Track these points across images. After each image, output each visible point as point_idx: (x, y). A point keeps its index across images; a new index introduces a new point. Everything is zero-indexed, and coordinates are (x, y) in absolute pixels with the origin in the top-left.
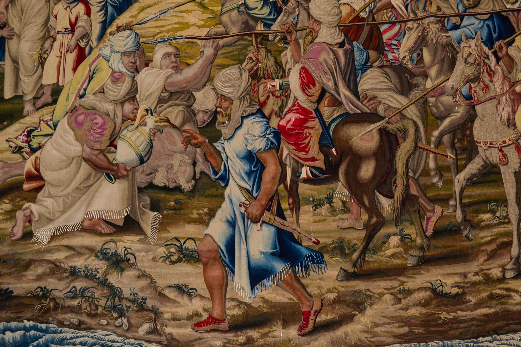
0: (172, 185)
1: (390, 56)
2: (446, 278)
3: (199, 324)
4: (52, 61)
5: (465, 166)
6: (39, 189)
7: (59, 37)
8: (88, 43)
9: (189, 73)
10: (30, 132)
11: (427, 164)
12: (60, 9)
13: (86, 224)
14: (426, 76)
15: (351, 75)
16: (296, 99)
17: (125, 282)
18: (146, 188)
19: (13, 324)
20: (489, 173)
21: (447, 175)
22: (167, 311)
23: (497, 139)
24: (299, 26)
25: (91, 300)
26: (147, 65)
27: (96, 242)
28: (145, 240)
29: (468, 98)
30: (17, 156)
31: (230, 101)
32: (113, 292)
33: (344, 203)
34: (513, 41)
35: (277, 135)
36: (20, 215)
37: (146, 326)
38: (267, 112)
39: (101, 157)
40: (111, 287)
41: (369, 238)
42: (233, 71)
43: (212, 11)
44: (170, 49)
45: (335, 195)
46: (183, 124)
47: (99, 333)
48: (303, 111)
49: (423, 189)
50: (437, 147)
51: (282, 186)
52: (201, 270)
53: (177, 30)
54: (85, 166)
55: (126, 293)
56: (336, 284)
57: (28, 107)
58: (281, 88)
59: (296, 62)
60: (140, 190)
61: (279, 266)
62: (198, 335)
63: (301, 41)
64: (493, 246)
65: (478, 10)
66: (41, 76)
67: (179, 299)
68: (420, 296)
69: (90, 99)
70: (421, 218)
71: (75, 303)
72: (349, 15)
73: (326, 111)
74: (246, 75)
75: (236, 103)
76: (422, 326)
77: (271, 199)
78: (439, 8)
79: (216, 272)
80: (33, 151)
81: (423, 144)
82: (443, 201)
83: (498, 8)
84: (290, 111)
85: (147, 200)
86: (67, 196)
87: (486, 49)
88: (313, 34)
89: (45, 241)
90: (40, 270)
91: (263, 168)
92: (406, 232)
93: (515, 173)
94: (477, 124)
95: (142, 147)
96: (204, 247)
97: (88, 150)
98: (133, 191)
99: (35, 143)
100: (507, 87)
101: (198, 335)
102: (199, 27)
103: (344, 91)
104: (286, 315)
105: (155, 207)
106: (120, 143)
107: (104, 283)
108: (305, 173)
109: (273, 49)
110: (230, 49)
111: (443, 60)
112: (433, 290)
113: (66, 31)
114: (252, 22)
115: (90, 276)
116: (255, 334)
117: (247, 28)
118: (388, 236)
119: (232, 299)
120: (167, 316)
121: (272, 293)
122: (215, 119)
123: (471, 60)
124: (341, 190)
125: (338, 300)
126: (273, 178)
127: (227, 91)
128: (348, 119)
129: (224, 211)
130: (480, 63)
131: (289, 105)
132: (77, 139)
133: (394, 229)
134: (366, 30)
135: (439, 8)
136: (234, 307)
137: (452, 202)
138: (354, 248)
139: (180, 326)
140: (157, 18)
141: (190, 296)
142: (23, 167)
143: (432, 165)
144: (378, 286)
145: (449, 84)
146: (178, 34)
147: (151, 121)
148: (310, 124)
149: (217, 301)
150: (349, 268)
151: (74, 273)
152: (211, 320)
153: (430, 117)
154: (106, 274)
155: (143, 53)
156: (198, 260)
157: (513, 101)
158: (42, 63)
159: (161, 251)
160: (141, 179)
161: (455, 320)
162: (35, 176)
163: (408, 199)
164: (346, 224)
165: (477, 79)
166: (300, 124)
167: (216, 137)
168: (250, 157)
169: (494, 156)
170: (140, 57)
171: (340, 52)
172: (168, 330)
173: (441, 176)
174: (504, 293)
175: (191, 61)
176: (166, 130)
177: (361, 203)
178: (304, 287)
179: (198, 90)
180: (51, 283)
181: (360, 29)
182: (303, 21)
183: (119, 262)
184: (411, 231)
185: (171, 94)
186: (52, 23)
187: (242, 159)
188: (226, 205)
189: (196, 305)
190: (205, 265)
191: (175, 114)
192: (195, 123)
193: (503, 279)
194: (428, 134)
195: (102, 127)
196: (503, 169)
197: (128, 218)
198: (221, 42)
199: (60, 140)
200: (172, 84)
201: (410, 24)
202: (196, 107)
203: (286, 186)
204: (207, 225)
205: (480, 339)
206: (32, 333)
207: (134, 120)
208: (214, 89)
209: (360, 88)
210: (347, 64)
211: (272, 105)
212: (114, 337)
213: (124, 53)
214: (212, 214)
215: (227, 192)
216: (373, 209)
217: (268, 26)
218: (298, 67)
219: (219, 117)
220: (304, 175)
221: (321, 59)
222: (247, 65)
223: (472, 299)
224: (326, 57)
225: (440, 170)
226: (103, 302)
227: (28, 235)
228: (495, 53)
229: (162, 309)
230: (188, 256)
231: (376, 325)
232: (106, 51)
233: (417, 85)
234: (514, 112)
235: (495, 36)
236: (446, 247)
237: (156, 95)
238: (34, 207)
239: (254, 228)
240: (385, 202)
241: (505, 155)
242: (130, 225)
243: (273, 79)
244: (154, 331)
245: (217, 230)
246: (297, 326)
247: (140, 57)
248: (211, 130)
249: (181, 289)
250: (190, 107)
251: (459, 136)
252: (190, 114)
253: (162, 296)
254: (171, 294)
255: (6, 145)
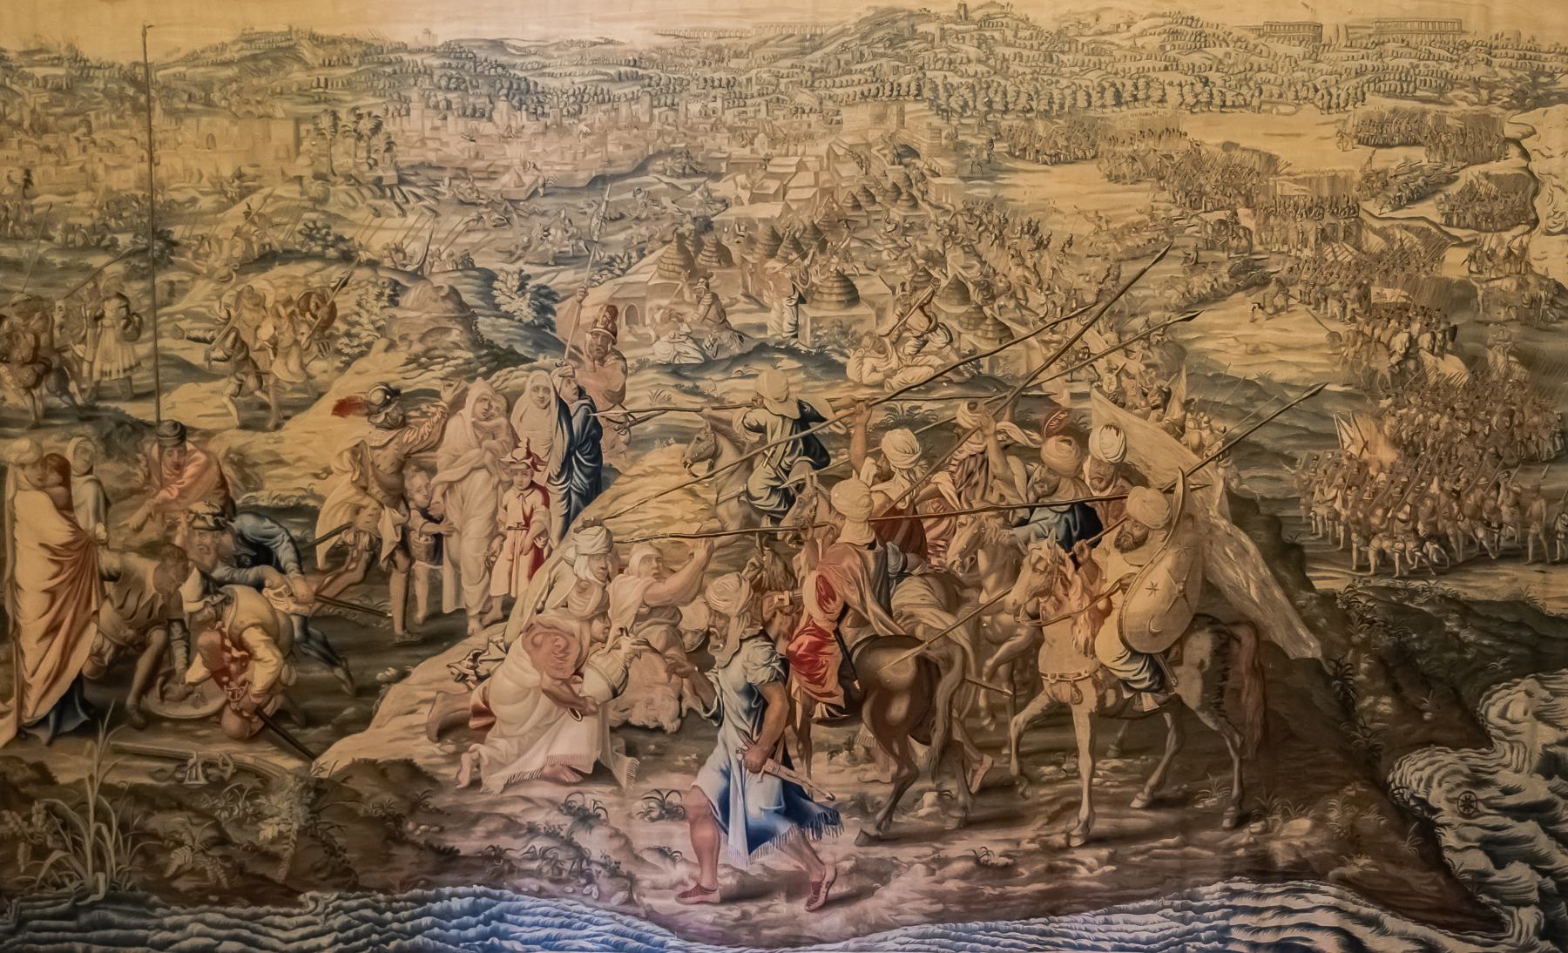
0: (652, 725)
1: (934, 561)
2: (992, 844)
3: (684, 895)
4: (501, 566)
5: (1024, 706)
6: (488, 727)
7: (510, 534)
8: (546, 543)
9: (674, 582)
10: (476, 656)
11: (976, 701)
12: (510, 497)
13: (547, 770)
14: (979, 587)
15: (883, 586)
16: (810, 617)
17: (595, 843)
18: (620, 727)
19: (461, 889)
20: (1058, 715)
21: (1001, 716)
22: (646, 878)
23: (1071, 671)
24: (817, 521)
25: (555, 863)
26: (621, 571)
27: (560, 793)
28: (620, 791)
29: (1035, 616)
30: (461, 687)
31: (727, 618)
32: (581, 854)
33: (868, 750)
34: (1099, 541)
35: (785, 663)
36: (466, 759)
37: (621, 895)
38: (772, 633)
39: (565, 688)
40: (578, 848)
41: (898, 794)
42: (731, 580)
43: (705, 501)
44: (650, 552)
45: (857, 740)
46: (668, 646)
47: (564, 902)
48: (820, 632)
49: (970, 733)
50: (990, 680)
51: (790, 728)
52: (688, 830)
53: (659, 526)
54: (545, 701)
55: (596, 855)
56: (855, 849)
57: (473, 625)
58: (791, 603)
59: (812, 569)
60: (612, 730)
61: (784, 827)
62: (682, 907)
63: (819, 541)
64: (1057, 807)
65: (1055, 499)
66: (488, 585)
67: (661, 866)
68: (959, 866)
69: (550, 615)
70: (965, 771)
71: (534, 865)
72: (882, 506)
73: (848, 631)
74: (746, 586)
75: (734, 621)
76: (958, 903)
77: (776, 744)
78: (1002, 497)
79: (706, 832)
80: (481, 679)
81: (971, 677)
82: (994, 749)
83: (1081, 497)
84: (802, 632)
85: (621, 743)
86: (522, 736)
87: (1062, 551)
88: (835, 532)
89: (497, 791)
90: (492, 826)
91: (766, 705)
92: (947, 787)
93: (1091, 715)
94: (1044, 651)
95: (616, 677)
96: (690, 801)
97: (547, 679)
98: (604, 734)
99: (482, 670)
100: (1086, 603)
101: (682, 907)
102: (688, 522)
103: (873, 608)
104: (794, 887)
105: (631, 751)
106: (587, 671)
107: (569, 843)
108: (819, 711)
109: (782, 551)
110: (726, 552)
111: (1004, 566)
112: (977, 860)
113: (518, 527)
114: (754, 516)
115: (552, 834)
116: (751, 907)
117: (749, 523)
118: (922, 792)
119: (725, 866)
120: (646, 884)
121: (776, 860)
122: (707, 641)
123: (1041, 566)
124: (865, 732)
125: (857, 870)
126: (779, 718)
127: (721, 606)
128: (876, 643)
129: (717, 758)
130: (1054, 572)
131: (802, 624)
132: (535, 665)
133: (930, 784)
134: (905, 526)
135: (1002, 497)
136: (726, 875)
137: (1005, 751)
138: (878, 806)
139: (660, 897)
140: (633, 510)
141: (674, 860)
142: (468, 699)
143: (982, 703)
144: (906, 853)
145: (1010, 599)
146: (661, 532)
147: (627, 644)
148: (827, 649)
149: (707, 868)
150: (872, 831)
151: (532, 830)
152: (700, 890)
153: (983, 641)
154: (571, 832)
155: (616, 555)
156: (683, 817)
157: (1093, 621)
158: (489, 567)
159: (639, 805)
160: (614, 717)
161: (1003, 897)
162: (483, 712)
163: (948, 746)
164: (869, 776)
165: (1047, 592)
166: (815, 648)
167: (709, 664)
168: (750, 691)
169: (1065, 693)
170: (613, 560)
171: (870, 555)
172: (646, 901)
173: (994, 717)
174: (1068, 864)
175: (675, 567)
176: (645, 655)
177: (890, 751)
178: (815, 853)
179: (686, 604)
180: (504, 841)
181: (896, 524)
182: (823, 515)
183: (586, 818)
184: (952, 786)
185: (653, 609)
186: (500, 516)
187: (739, 693)
188: (719, 750)
189: (680, 871)
190: (692, 824)
191: (657, 634)
192: (682, 646)
193: (1067, 848)
194: (980, 664)
195: (565, 650)
196: (1075, 709)
197: (597, 765)
198: (717, 541)
199: (514, 667)
200: (654, 597)
201: (962, 518)
202: (683, 626)
203: (794, 728)
204: (696, 775)
205: (1032, 920)
206: (484, 900)
207: (605, 642)
208: (707, 603)
209: (894, 604)
210: (878, 570)
211: (779, 624)
212: (581, 907)
213: (591, 556)
214: (701, 761)
215: (720, 734)
216: (905, 758)
217: (776, 521)
218: (815, 574)
219: (712, 638)
220: (817, 715)
221: (844, 565)
222: (747, 572)
223: (1025, 872)
224: (852, 562)
225: (993, 710)
226: (568, 866)
227: (476, 783)
228: (1074, 558)
229: (638, 876)
230: (671, 813)
231: (902, 901)
232: (571, 554)
233: (967, 600)
234: (1094, 636)
235: (1075, 534)
236: (997, 805)
237: (632, 612)
238: (483, 750)
239: (753, 780)
240: (920, 751)
241: (1078, 691)
242: (601, 772)
243: (781, 591)
244: (629, 901)
245: (708, 781)
246: (804, 900)
247: (613, 560)
248: (701, 655)
249: (664, 852)
250: (675, 626)
251: (1020, 666)
252: (675, 635)
253: (638, 859)
254: (651, 858)
255: (447, 672)
